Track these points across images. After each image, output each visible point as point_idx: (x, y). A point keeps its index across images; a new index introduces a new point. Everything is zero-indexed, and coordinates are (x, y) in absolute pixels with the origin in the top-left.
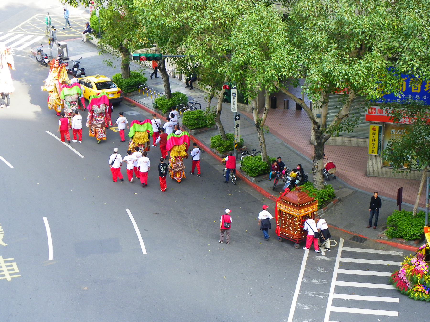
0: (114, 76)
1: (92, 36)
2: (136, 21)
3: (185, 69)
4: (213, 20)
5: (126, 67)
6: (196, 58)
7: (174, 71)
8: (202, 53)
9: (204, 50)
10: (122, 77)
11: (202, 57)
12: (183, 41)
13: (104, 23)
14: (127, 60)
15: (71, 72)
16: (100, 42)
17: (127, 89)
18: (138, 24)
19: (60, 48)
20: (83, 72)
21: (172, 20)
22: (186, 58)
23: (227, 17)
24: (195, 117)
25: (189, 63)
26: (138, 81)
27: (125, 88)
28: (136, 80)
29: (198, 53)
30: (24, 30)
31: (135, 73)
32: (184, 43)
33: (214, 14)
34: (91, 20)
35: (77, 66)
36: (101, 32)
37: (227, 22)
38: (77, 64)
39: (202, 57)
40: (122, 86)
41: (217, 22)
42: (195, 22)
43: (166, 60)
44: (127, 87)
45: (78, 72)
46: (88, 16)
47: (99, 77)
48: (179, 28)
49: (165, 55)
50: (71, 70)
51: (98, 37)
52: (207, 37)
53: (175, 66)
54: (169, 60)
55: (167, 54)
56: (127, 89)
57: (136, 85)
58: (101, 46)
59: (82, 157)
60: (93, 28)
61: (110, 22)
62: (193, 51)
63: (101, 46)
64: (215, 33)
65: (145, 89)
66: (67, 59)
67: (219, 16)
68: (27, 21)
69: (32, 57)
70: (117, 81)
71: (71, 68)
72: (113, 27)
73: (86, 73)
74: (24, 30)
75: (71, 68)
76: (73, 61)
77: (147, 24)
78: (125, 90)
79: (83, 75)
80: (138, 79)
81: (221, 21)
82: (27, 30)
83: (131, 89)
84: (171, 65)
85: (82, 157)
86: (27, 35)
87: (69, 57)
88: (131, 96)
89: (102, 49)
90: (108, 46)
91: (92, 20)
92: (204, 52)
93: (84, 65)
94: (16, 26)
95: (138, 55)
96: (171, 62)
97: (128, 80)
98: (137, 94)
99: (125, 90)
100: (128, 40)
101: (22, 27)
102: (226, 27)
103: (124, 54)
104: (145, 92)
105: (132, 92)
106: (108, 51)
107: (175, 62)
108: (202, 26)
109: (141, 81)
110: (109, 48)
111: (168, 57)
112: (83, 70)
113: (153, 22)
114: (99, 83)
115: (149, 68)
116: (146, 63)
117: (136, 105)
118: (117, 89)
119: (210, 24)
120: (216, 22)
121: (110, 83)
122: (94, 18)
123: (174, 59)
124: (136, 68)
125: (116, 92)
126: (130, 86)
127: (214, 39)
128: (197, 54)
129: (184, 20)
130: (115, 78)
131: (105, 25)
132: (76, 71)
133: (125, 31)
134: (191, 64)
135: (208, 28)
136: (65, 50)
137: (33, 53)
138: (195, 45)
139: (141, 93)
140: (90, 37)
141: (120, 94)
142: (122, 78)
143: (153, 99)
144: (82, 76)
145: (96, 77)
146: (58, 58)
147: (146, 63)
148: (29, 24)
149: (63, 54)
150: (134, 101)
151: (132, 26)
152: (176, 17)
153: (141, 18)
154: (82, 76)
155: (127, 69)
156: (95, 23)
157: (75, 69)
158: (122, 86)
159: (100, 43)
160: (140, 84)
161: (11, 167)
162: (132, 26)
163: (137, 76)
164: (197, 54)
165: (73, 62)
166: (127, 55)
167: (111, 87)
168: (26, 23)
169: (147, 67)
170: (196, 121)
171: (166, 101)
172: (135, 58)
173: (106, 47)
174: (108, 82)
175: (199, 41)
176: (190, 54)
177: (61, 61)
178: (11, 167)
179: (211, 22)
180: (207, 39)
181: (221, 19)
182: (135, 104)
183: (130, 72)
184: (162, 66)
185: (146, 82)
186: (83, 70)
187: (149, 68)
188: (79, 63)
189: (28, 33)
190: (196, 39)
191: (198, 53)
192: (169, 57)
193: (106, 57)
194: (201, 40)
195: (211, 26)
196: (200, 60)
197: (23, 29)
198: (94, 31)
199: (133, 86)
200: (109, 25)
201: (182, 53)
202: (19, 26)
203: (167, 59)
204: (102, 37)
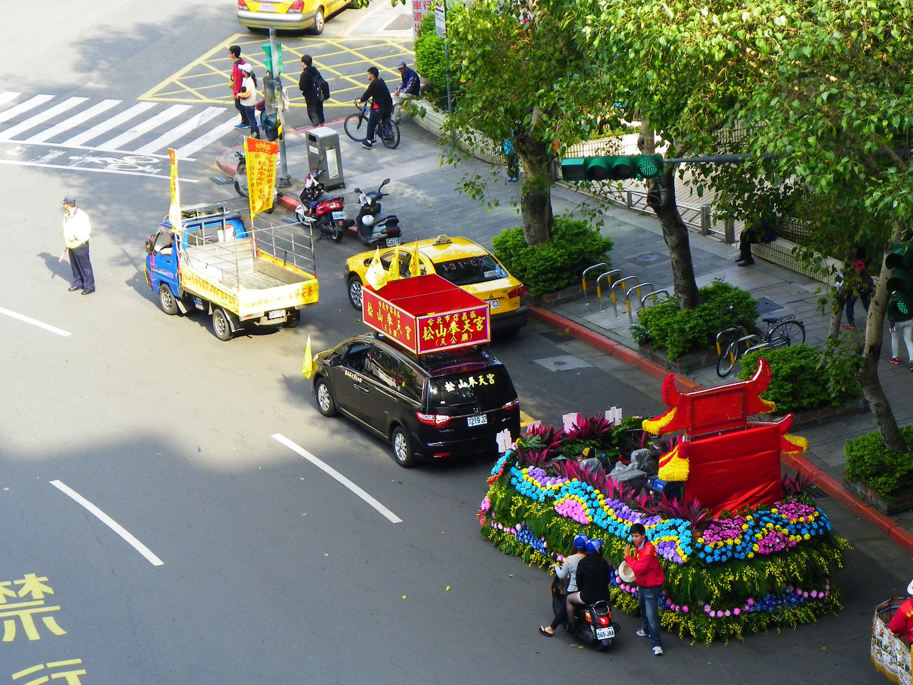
0: (499, 237)
1: (422, 104)
2: (570, 44)
3: (746, 205)
4: (845, 28)
5: (537, 204)
6: (784, 161)
7: (705, 213)
8: (808, 145)
9: (812, 132)
10: (527, 240)
11: (805, 158)
12: (737, 106)
13: (462, 58)
14: (538, 182)
15: (354, 228)
16: (451, 123)
17: (544, 281)
18: (580, 56)
19: (315, 150)
20: (394, 230)
21: (698, 34)
22: (747, 165)
23: (895, 15)
24: (785, 369)
25: (761, 182)
26: (581, 251)
27: (536, 276)
28: (573, 248)
29: (790, 143)
30: (192, 91)
31: (569, 227)
32: (742, 113)
33: (848, 8)
34: (417, 47)
35: (373, 209)
36: (452, 89)
37: (895, 32)
38: (373, 201)
39: (805, 158)
40: (524, 270)
41: (860, 34)
42: (779, 36)
43: (677, 174)
44: (543, 273)
45: (376, 229)
46: (410, 35)
47: (449, 242)
48: (723, 62)
49: (673, 160)
50: (352, 223)
51: (441, 105)
52: (822, 88)
53: (710, 195)
54: (688, 175)
55: (681, 155)
56: (544, 281)
57: (573, 266)
58: (453, 137)
59: (394, 519)
60: (426, 76)
61: (483, 55)
62: (770, 139)
63: (453, 137)
64: (852, 74)
65: (605, 278)
66: (339, 185)
67: (864, 12)
68: (201, 60)
69: (219, 183)
70: (508, 255)
71: (354, 218)
72: (494, 71)
73: (403, 230)
74: (192, 91)
75: (354, 218)
76: (358, 191)
77: (609, 51)
78: (536, 283)
79: (394, 240)
80: (580, 246)
81: (872, 29)
82: (200, 92)
83: (555, 280)
84: (695, 192)
85: (394, 519)
86: (204, 107)
87: (345, 181)
88: (557, 304)
89: (455, 143)
90: (478, 135)
91: (421, 49)
92: (811, 140)
93: (396, 206)
94: (163, 78)
95: (581, 162)
96: (695, 182)
97: (547, 251)
98: (579, 298)
99: (536, 283)
100: (545, 111)
101: (185, 82)
102: (890, 50)
103: (530, 162)
104: (605, 287)
105: (558, 289)
106: (477, 152)
107: (709, 180)
108: (807, 51)
109: (591, 252)
110: (479, 141)
111: (683, 166)
112: (393, 222)
113: (630, 46)
114: (447, 263)
115: (619, 206)
116: (606, 189)
117: (574, 335)
118: (507, 282)
119: (835, 42)
120: (854, 34)
121: (485, 263)
122: (430, 40)
123: (705, 171)
124: (571, 209)
125: (505, 291)
126: (553, 270)
127: (851, 94)
128: (789, 148)
129: (741, 33)
130: (502, 246)
131: (465, 63)
132: (371, 227)
133: (532, 82)
134: (768, 184)
135: (826, 57)
136: (331, 155)
137: (225, 170)
138: (781, 116)
139: (592, 293)
140: (414, 107)
141: (517, 299)
142: (526, 245)
143: (634, 313)
144: (389, 241)
145: (439, 243)
146: (308, 184)
147: (606, 189)
148: (206, 70)
149: (326, 170)
150: (567, 322)
151: (558, 61)
152: (711, 24)
153: (588, 30)
154: (389, 241)
155: (542, 213)
156: (430, 58)
157: (367, 220)
158: (524, 270)
159: (450, 126)
160: (587, 263)
161: (156, 561)
162: (558, 61)
163: (577, 235)
164: (789, 148)
165: (361, 197)
166: (540, 162)
167: (487, 274)
168: (200, 65)
169: (610, 202)
170: (789, 387)
171: (678, 318)
172: (571, 173)
173: (469, 139)
174: (476, 259)
175: (796, 103)
176: (764, 149)
177: (320, 194)
178: (156, 561)
179: (837, 34)
180: (825, 96)
181: (875, 24)
182: (573, 331)
183: (551, 221)
184: (663, 197)
185: (608, 253)
186: (393, 222)
187: (619, 206)
188: (380, 196)
189: (206, 100)
190: (784, 95)
191: (790, 143)
192: (689, 163)
193: (468, 171)
194: (801, 97)
195: (838, 49)
196: (799, 169)
197: (188, 89)
198: (430, 88)
199: (561, 270)
200: (479, 63)
201: (735, 147)
202: (175, 78)
203: (682, 172)
204: (454, 104)
